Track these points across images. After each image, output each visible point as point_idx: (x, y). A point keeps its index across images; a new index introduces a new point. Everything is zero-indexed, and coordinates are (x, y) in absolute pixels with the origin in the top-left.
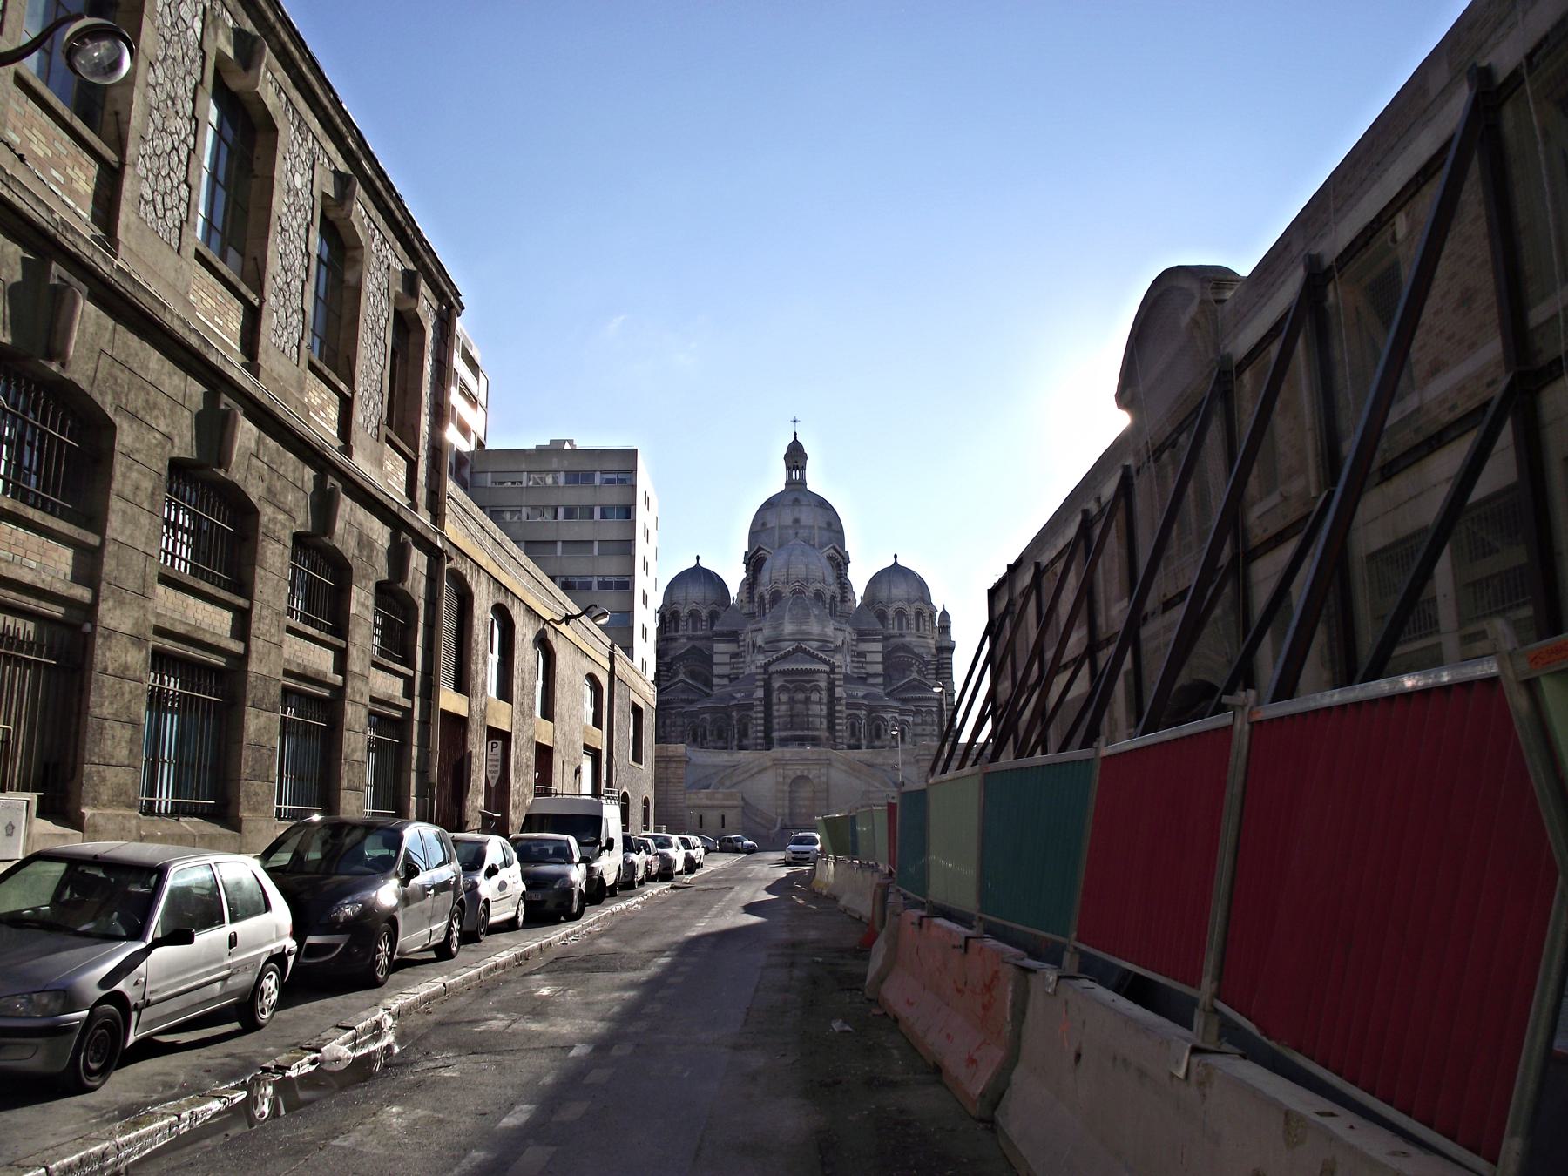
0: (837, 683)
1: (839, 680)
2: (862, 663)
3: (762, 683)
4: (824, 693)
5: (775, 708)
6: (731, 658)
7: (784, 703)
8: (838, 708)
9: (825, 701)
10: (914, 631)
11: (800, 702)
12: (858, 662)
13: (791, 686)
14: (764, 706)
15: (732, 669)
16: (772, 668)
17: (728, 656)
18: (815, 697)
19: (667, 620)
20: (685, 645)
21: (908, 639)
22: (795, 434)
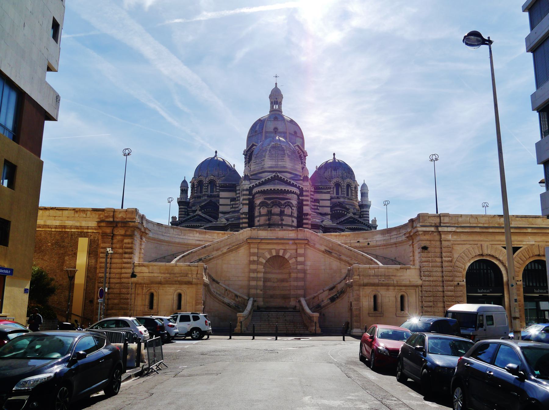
0: (304, 203)
1: (307, 200)
2: (317, 206)
3: (247, 202)
4: (295, 209)
5: (256, 219)
6: (231, 201)
7: (263, 215)
8: (305, 221)
9: (295, 215)
10: (345, 196)
11: (277, 215)
12: (315, 206)
13: (269, 202)
14: (248, 218)
15: (231, 208)
16: (255, 191)
17: (230, 200)
18: (288, 211)
19: (195, 186)
20: (205, 200)
21: (342, 200)
22: (276, 84)
